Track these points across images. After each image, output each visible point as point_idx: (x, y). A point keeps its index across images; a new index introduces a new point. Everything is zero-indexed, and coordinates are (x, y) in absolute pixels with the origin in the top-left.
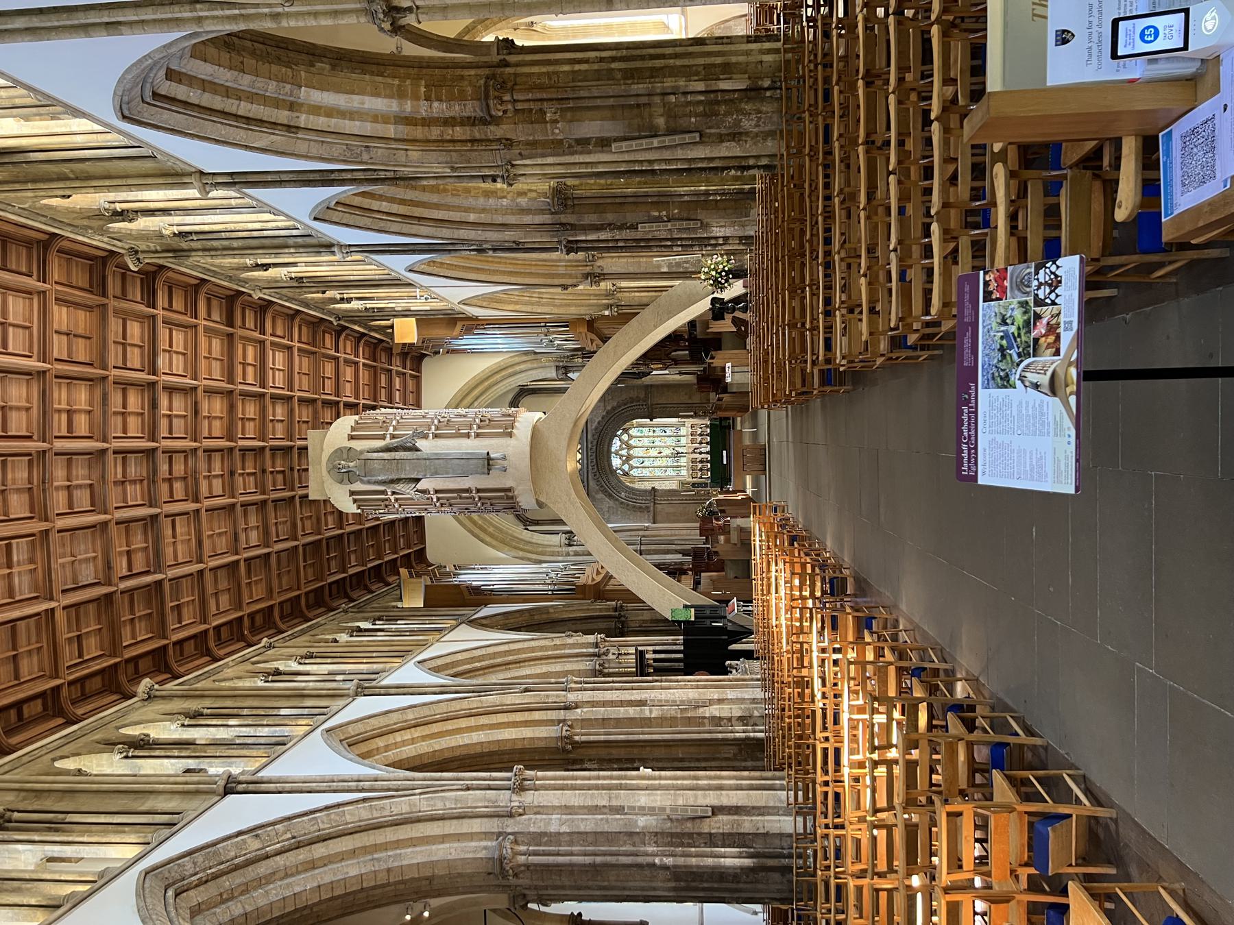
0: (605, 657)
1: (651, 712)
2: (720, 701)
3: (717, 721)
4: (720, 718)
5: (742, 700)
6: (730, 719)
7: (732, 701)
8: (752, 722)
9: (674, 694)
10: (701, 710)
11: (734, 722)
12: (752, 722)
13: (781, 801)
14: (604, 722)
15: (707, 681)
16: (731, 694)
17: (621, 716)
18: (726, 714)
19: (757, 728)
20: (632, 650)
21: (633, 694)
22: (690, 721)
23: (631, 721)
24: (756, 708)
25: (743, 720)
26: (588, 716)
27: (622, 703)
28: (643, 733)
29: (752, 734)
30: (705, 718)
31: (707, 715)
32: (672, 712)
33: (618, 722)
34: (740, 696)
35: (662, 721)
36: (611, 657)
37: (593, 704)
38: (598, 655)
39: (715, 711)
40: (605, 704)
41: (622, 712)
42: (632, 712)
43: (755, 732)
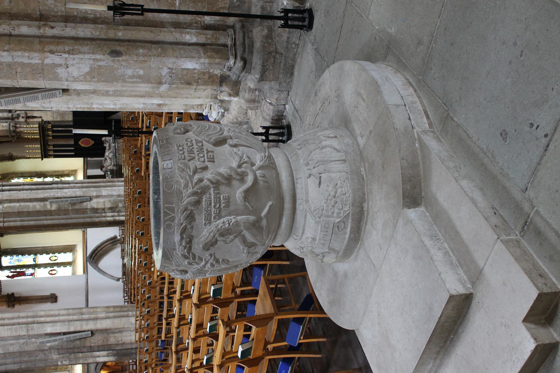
0: (16, 120)
1: (51, 206)
2: (97, 197)
3: (95, 210)
4: (97, 209)
5: (112, 196)
6: (104, 209)
7: (105, 196)
8: (117, 210)
9: (66, 193)
10: (85, 204)
11: (106, 211)
12: (117, 210)
13: (132, 324)
14: (19, 214)
15: (89, 183)
16: (104, 192)
17: (31, 210)
18: (101, 206)
19: (121, 214)
20: (37, 126)
21: (38, 194)
22: (77, 211)
23: (38, 213)
24: (120, 201)
25: (112, 209)
26: (7, 210)
27: (31, 200)
28: (46, 220)
29: (117, 218)
30: (87, 209)
31: (89, 207)
32: (66, 205)
33: (29, 214)
34: (110, 193)
35: (59, 211)
36: (21, 120)
37: (11, 201)
38: (12, 119)
39: (94, 204)
40: (18, 201)
41: (31, 206)
42: (38, 206)
43: (119, 216)
